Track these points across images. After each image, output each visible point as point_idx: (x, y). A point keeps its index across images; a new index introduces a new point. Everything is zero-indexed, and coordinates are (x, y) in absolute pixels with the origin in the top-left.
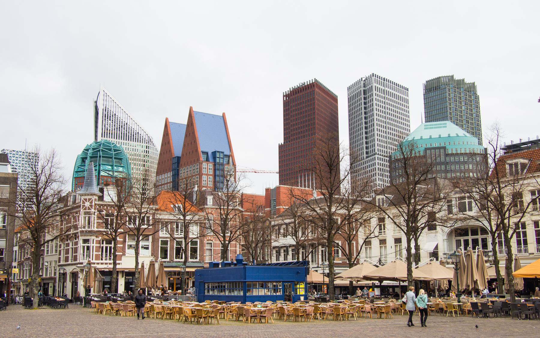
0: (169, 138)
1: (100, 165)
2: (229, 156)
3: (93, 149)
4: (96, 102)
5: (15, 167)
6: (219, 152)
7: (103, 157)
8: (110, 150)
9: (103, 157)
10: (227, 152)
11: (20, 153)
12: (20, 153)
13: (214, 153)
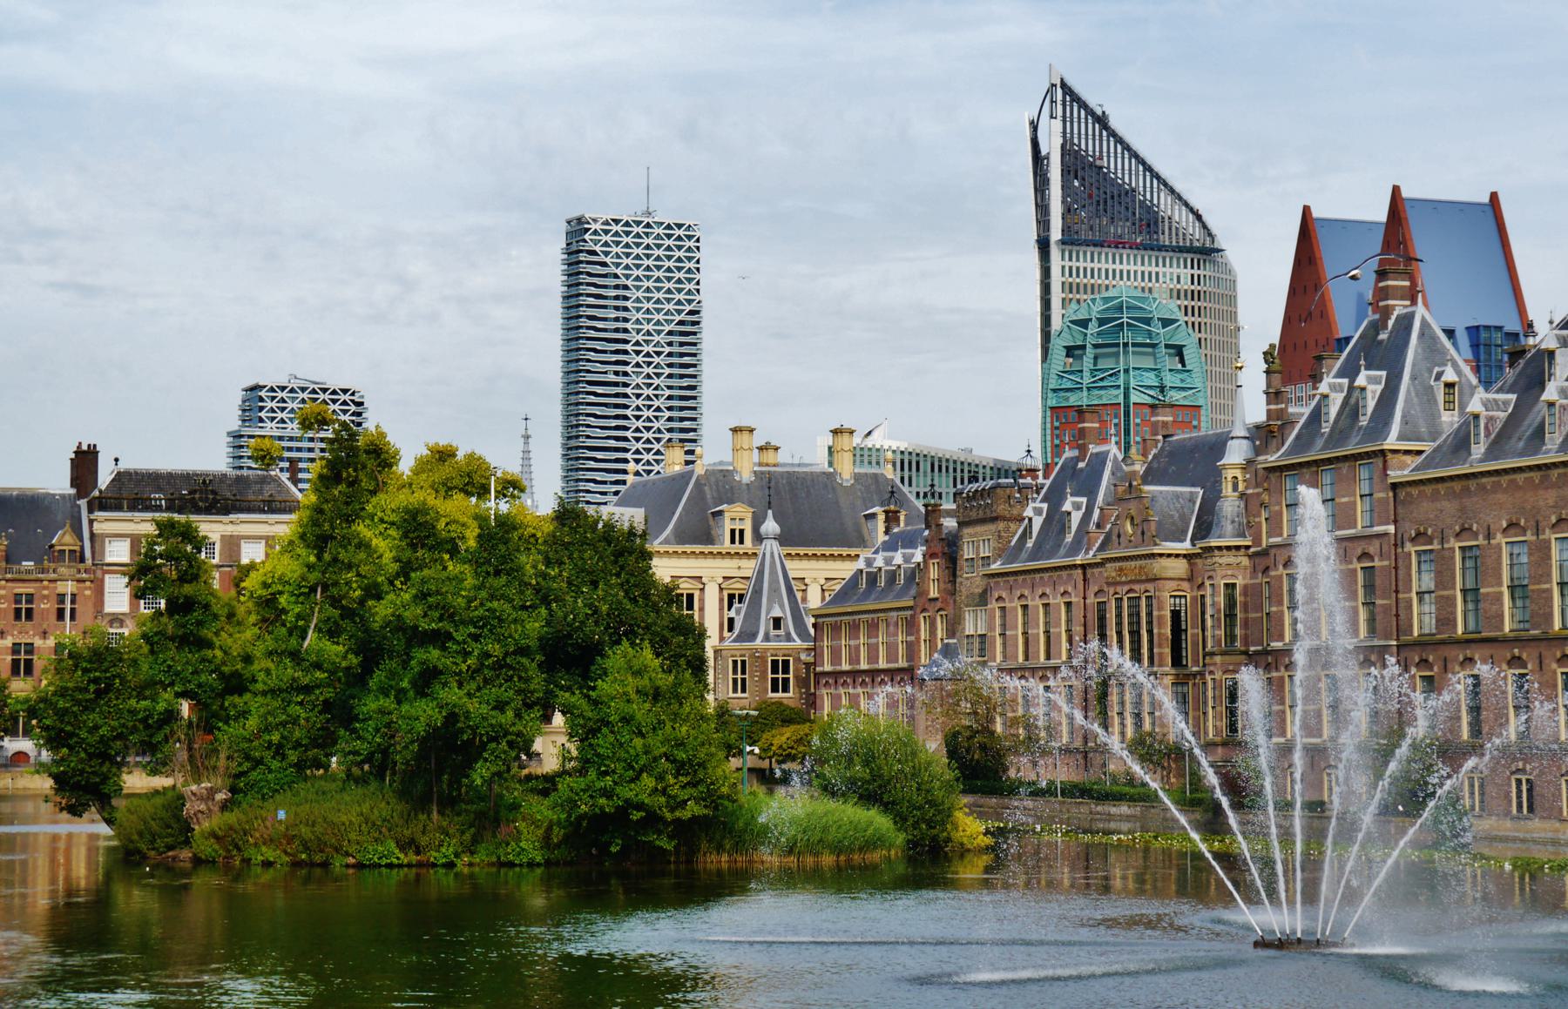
0: (1317, 272)
1: (1126, 371)
2: (1514, 336)
3: (1102, 322)
4: (1034, 127)
5: (623, 281)
6: (1487, 328)
7: (1134, 345)
8: (1148, 321)
9: (1134, 345)
10: (1513, 325)
11: (636, 229)
12: (636, 229)
13: (1473, 331)
